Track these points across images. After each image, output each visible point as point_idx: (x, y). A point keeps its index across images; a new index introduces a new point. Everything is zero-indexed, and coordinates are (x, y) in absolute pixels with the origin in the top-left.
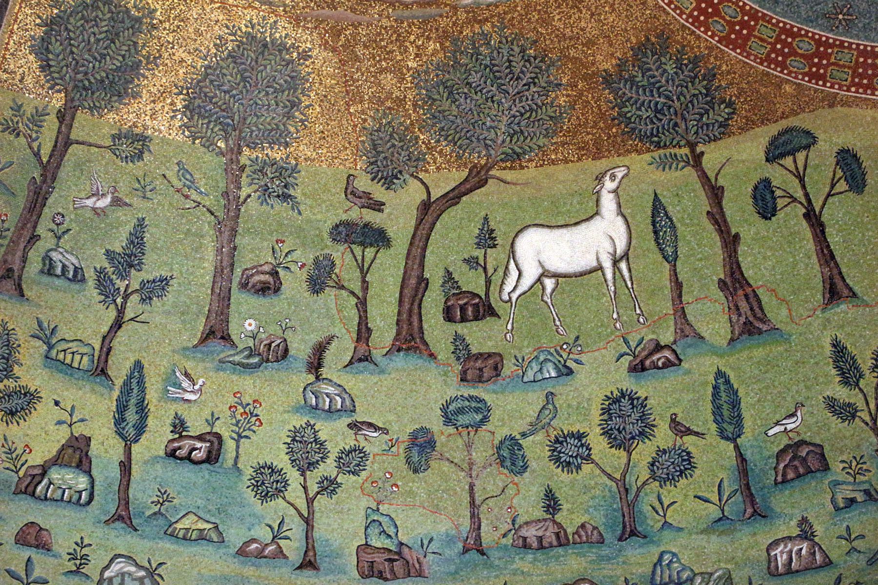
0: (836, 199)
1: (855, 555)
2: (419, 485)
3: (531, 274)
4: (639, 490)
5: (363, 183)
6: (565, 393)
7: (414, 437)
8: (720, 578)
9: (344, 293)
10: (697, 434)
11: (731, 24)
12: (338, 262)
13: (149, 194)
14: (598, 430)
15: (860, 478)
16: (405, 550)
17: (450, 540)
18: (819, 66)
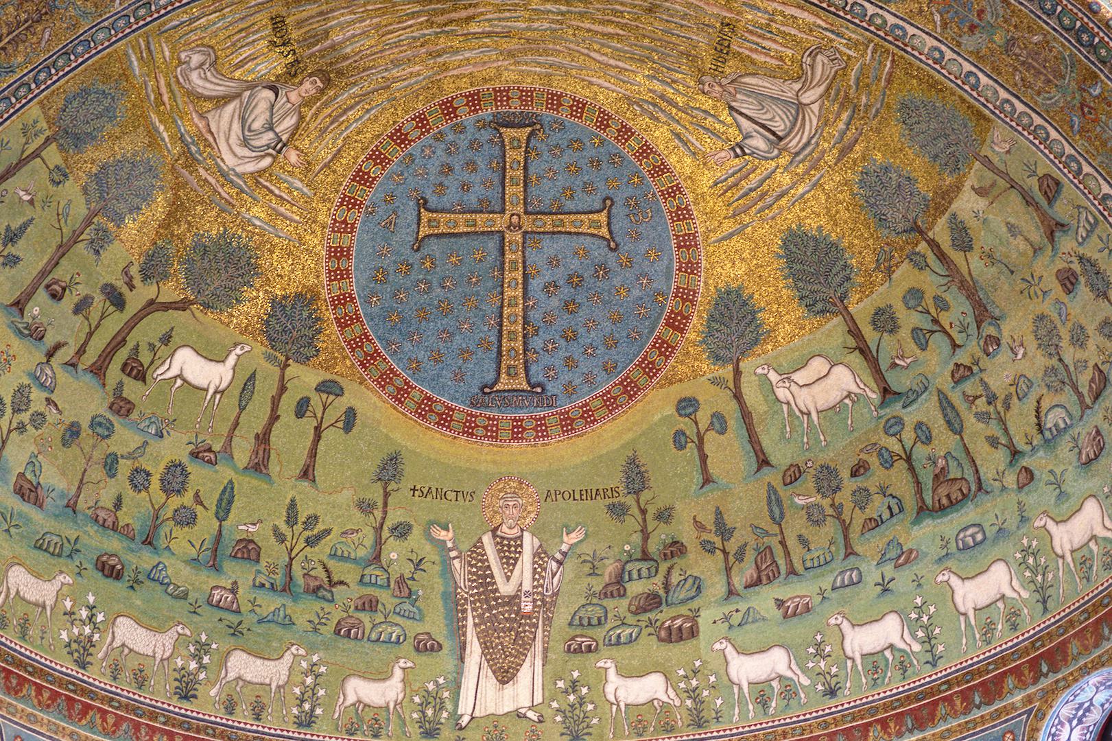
0: (334, 429)
1: (253, 614)
2: (61, 453)
3: (174, 371)
4: (163, 521)
5: (134, 271)
6: (155, 446)
7: (72, 425)
8: (183, 591)
9: (86, 322)
10: (205, 507)
11: (346, 315)
12: (95, 304)
13: (46, 208)
14: (158, 476)
15: (271, 575)
16: (39, 489)
17: (62, 496)
18: (368, 361)
